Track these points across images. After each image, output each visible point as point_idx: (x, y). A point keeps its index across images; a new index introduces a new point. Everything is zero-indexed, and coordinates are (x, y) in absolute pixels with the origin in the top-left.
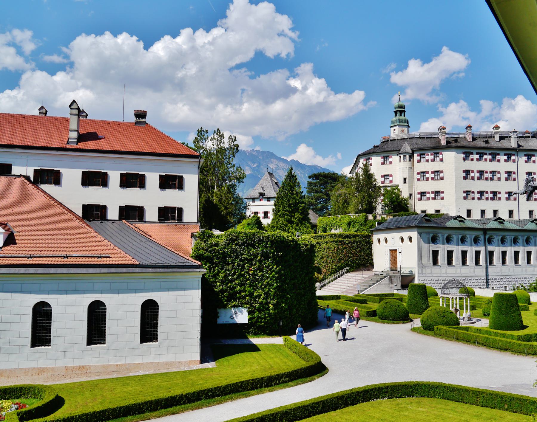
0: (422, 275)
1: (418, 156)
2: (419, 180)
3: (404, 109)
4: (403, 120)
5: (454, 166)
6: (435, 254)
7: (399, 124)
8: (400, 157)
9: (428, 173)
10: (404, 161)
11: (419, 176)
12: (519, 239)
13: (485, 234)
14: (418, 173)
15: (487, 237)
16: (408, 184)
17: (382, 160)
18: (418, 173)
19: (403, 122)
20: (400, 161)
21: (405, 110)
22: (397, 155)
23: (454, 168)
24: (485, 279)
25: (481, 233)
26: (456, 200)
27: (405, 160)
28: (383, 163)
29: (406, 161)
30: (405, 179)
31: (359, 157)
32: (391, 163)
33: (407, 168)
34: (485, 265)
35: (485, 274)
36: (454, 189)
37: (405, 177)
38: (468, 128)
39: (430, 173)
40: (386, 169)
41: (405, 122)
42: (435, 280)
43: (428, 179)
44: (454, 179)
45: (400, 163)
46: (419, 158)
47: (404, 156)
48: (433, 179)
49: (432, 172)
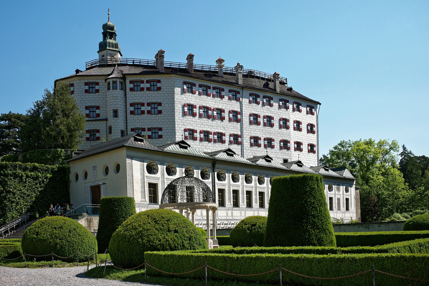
1: (131, 82)
2: (132, 113)
6: (153, 187)
8: (109, 84)
9: (143, 105)
10: (113, 89)
11: (132, 109)
14: (131, 105)
17: (87, 87)
18: (131, 105)
20: (109, 89)
22: (106, 80)
27: (115, 88)
28: (86, 91)
29: (116, 89)
31: (57, 83)
32: (97, 91)
39: (146, 105)
43: (143, 112)
45: (109, 91)
46: (132, 86)
48: (149, 112)
49: (149, 104)
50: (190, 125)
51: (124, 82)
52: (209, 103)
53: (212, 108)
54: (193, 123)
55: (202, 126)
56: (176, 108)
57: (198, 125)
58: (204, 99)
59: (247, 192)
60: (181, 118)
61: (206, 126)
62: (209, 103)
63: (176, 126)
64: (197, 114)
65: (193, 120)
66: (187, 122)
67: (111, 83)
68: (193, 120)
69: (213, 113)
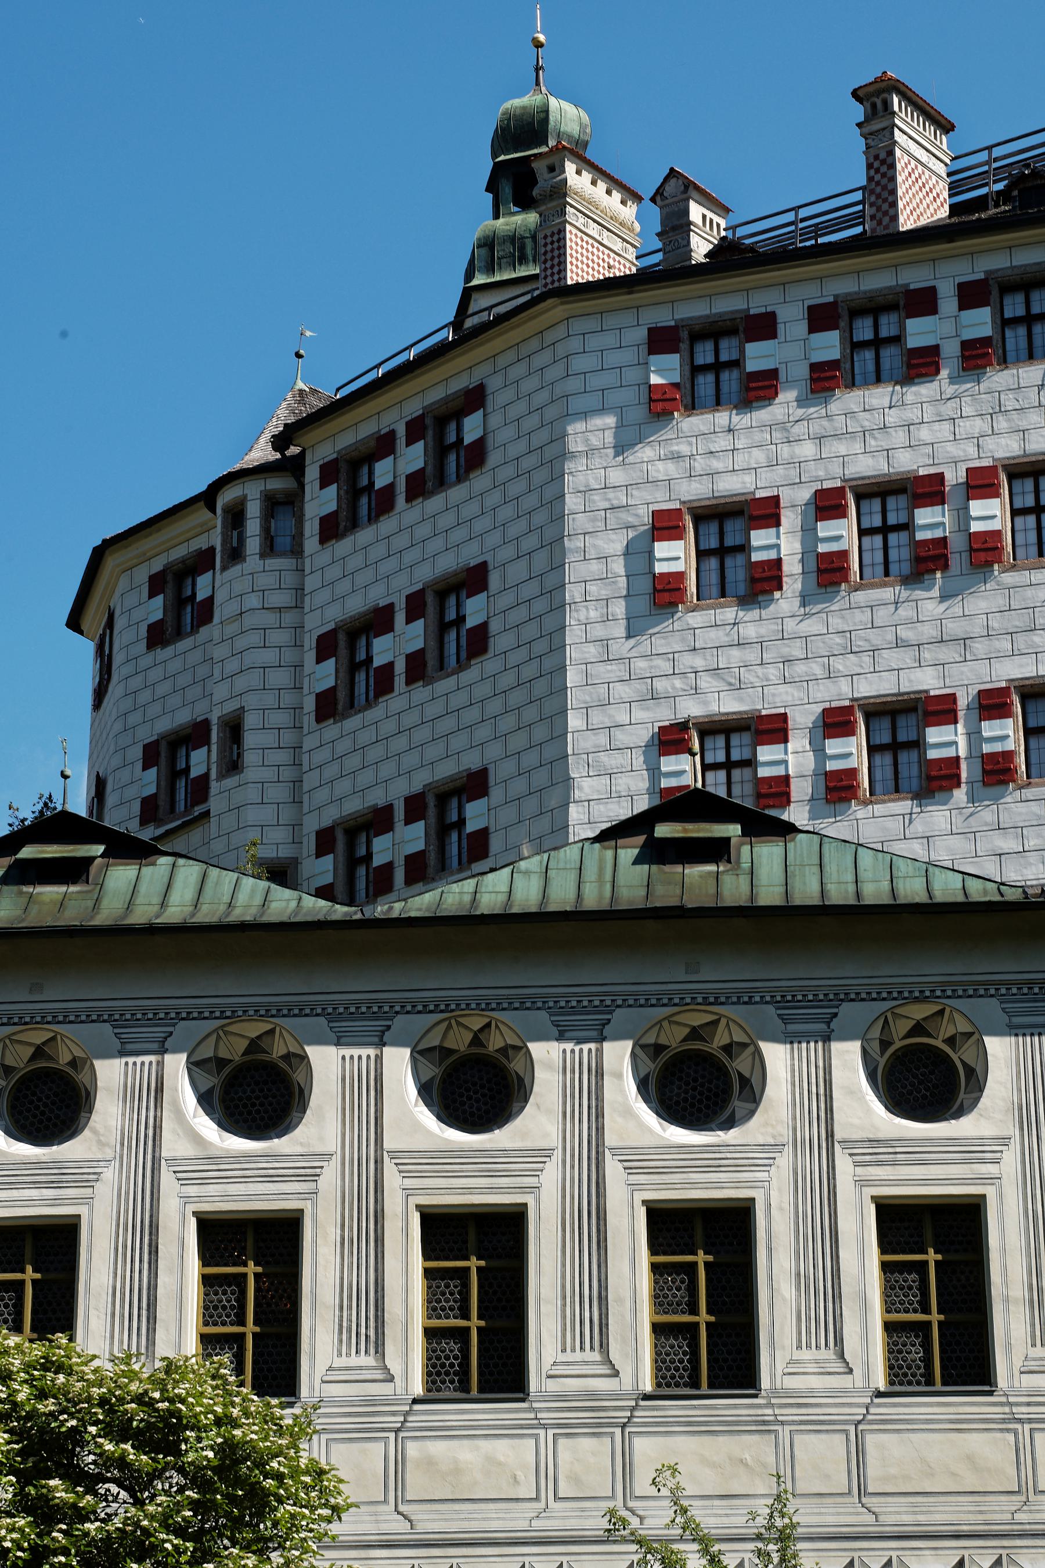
50: (718, 685)
52: (924, 434)
53: (954, 476)
54: (752, 655)
55: (839, 664)
56: (575, 570)
57: (800, 668)
58: (867, 421)
60: (622, 647)
61: (891, 658)
62: (924, 434)
63: (574, 721)
64: (792, 567)
65: (750, 631)
66: (689, 661)
68: (750, 631)
69: (963, 516)
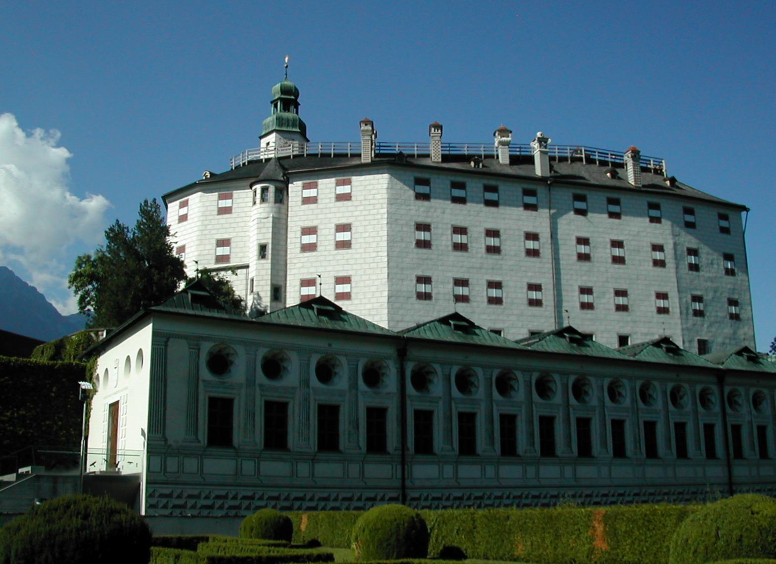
0: (161, 477)
3: (297, 96)
4: (288, 120)
5: (385, 210)
7: (277, 128)
8: (255, 192)
10: (263, 200)
12: (516, 379)
13: (402, 355)
15: (409, 367)
16: (269, 261)
19: (288, 126)
20: (255, 203)
21: (298, 100)
23: (386, 216)
24: (401, 498)
25: (389, 351)
26: (389, 299)
30: (263, 248)
33: (271, 220)
34: (400, 452)
35: (398, 484)
36: (386, 271)
37: (263, 242)
38: (433, 129)
40: (223, 227)
41: (294, 125)
42: (213, 495)
44: (384, 244)
47: (264, 190)
51: (286, 188)
59: (461, 415)
67: (259, 192)
